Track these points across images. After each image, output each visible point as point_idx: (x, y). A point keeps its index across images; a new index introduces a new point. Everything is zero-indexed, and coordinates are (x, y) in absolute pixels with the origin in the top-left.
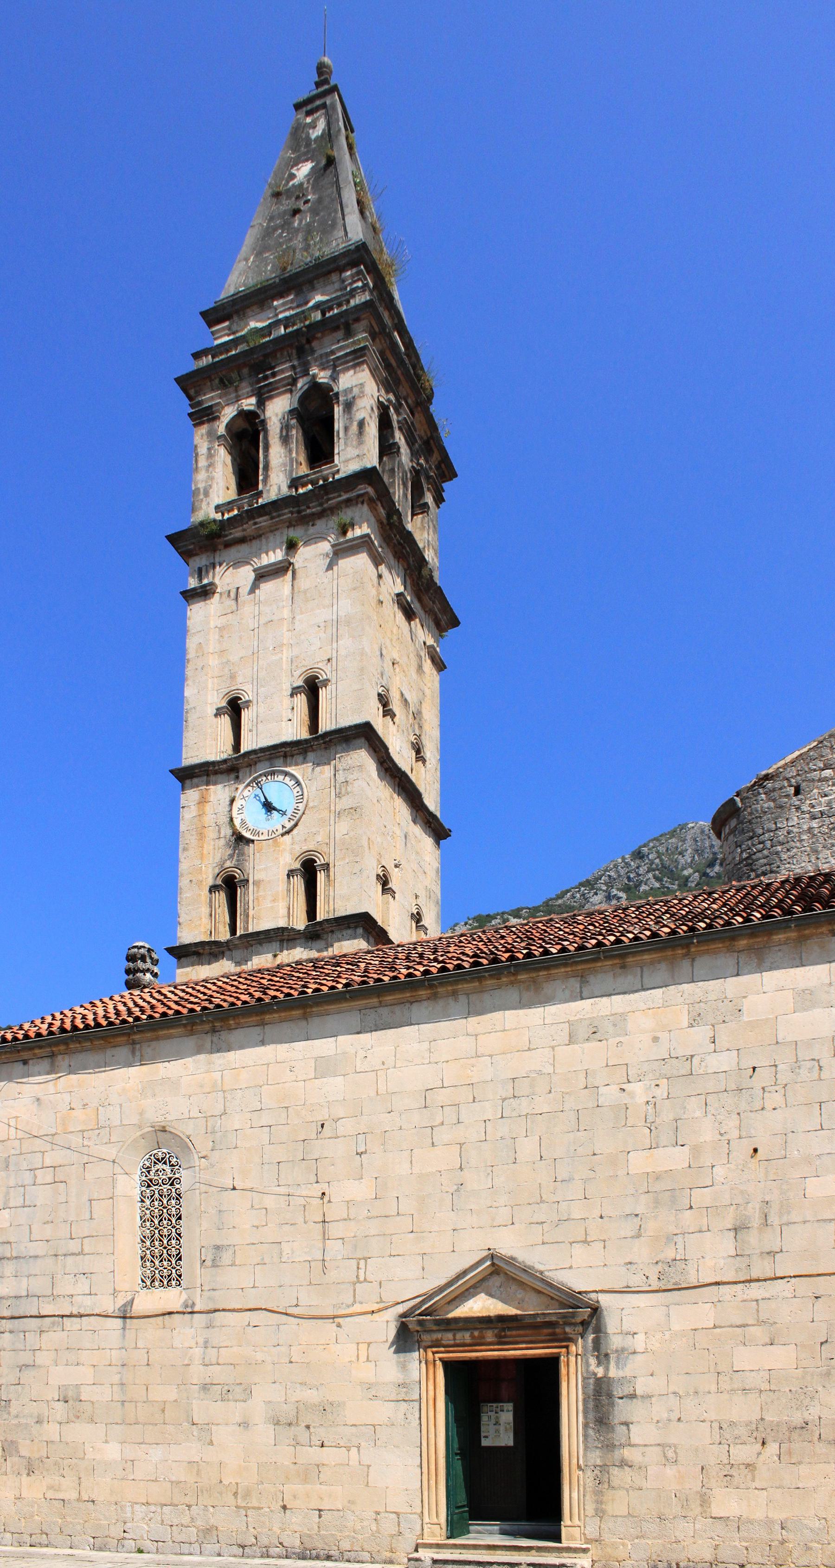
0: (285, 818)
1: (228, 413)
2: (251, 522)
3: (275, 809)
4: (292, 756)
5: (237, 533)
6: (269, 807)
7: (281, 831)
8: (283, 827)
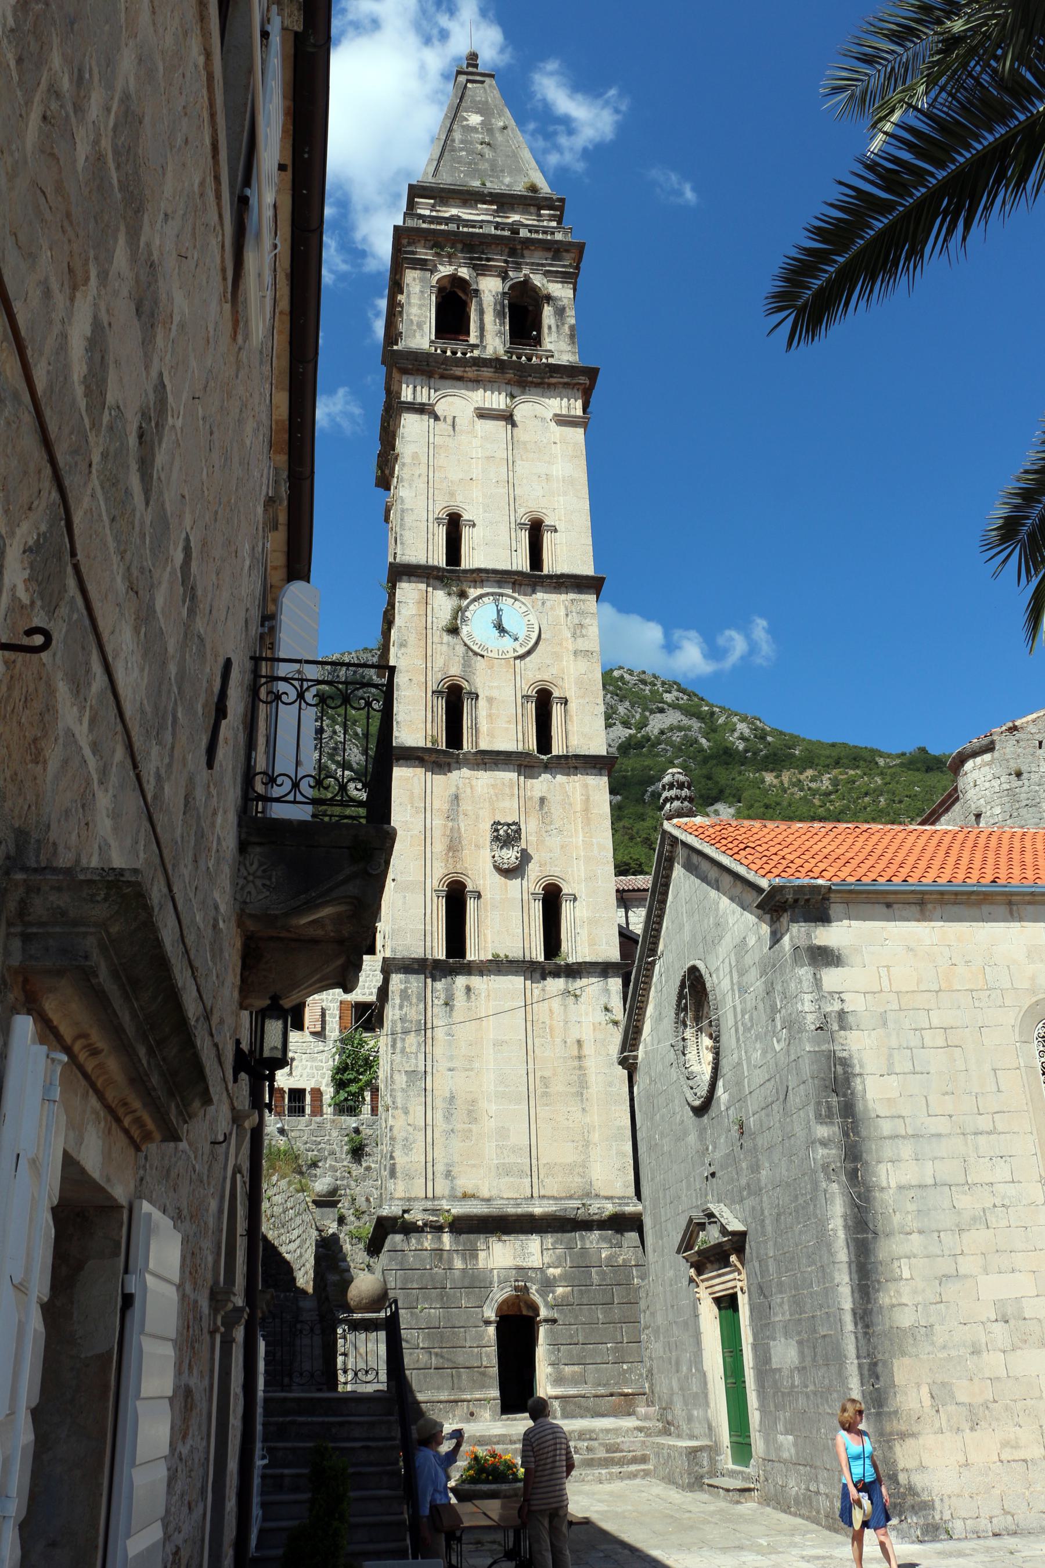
0: (517, 644)
1: (445, 270)
2: (474, 368)
3: (506, 632)
4: (520, 585)
5: (458, 371)
6: (500, 628)
7: (512, 654)
8: (515, 650)
